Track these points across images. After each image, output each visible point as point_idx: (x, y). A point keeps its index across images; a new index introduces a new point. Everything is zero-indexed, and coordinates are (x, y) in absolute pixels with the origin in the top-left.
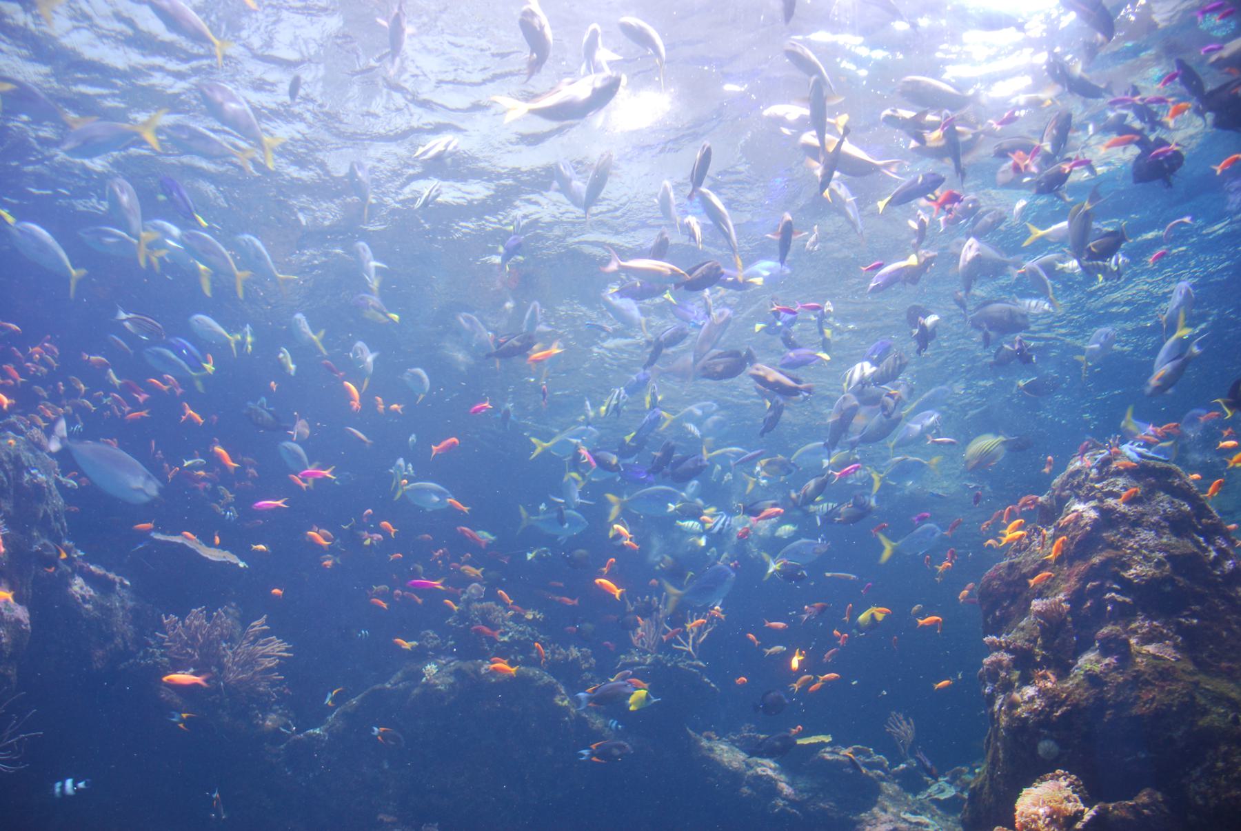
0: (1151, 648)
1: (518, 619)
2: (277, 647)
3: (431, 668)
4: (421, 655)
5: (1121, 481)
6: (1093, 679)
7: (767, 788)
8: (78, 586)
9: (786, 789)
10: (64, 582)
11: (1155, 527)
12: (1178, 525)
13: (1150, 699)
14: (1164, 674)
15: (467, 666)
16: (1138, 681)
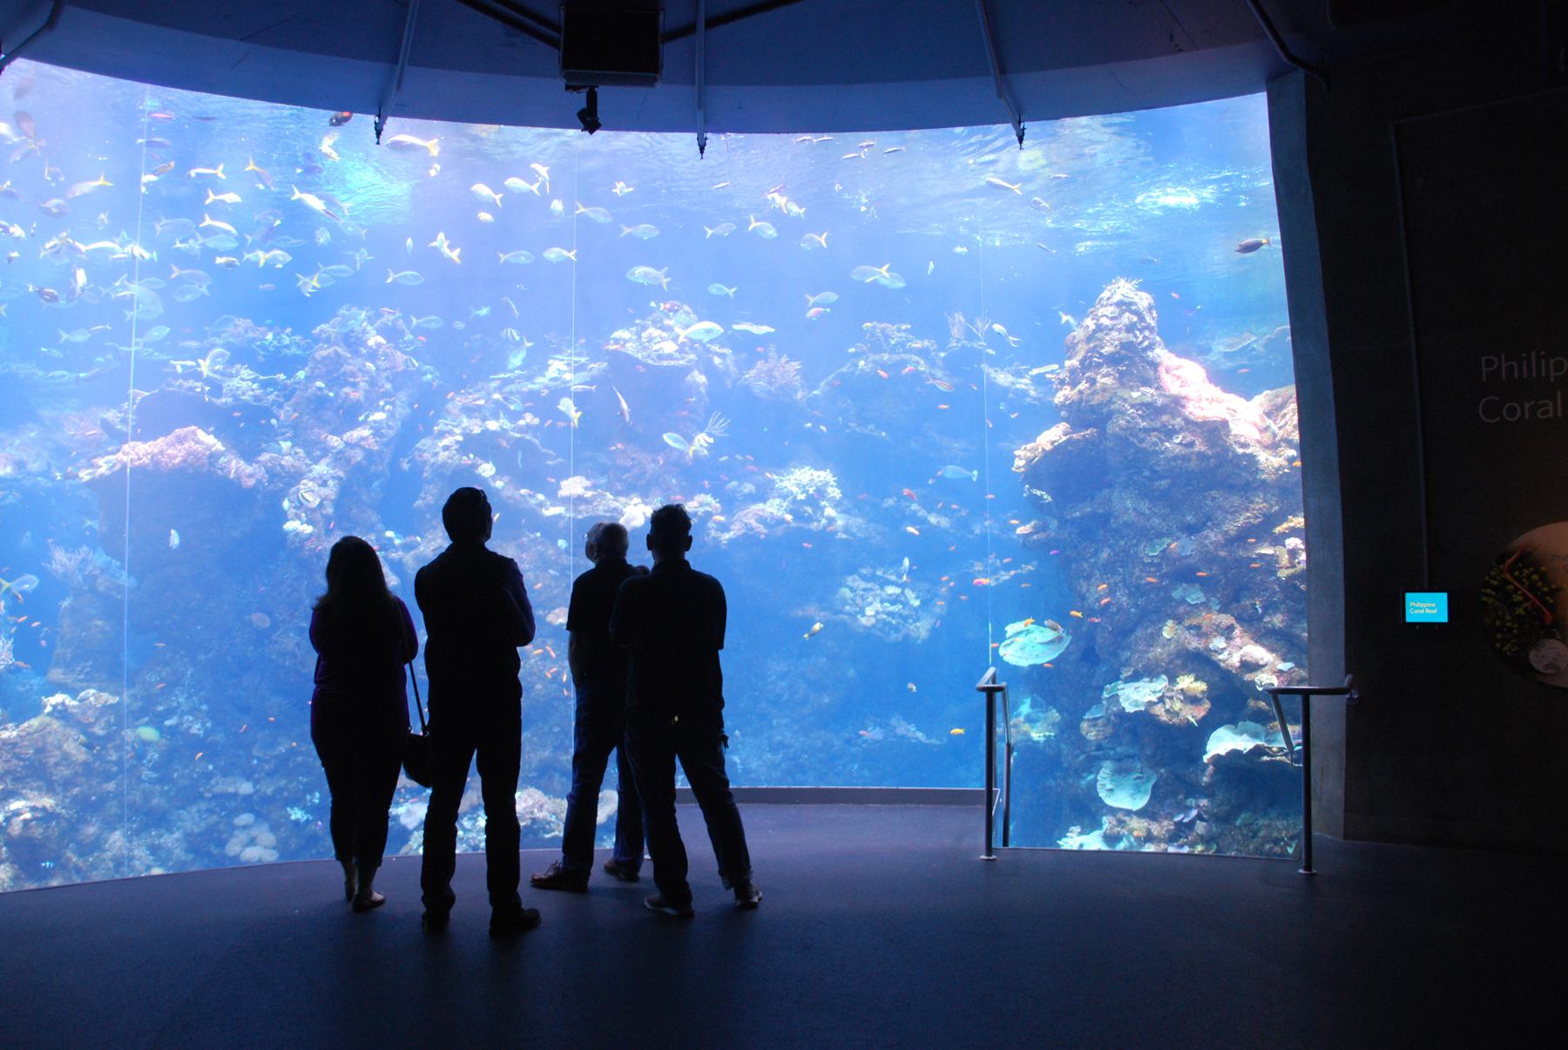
0: (1104, 380)
1: (899, 330)
2: (796, 365)
3: (862, 363)
4: (857, 355)
5: (1111, 309)
6: (1080, 392)
7: (1024, 393)
8: (717, 360)
9: (1033, 393)
10: (711, 361)
11: (1120, 330)
12: (1130, 328)
13: (1097, 399)
14: (1104, 390)
15: (877, 357)
16: (1095, 393)
